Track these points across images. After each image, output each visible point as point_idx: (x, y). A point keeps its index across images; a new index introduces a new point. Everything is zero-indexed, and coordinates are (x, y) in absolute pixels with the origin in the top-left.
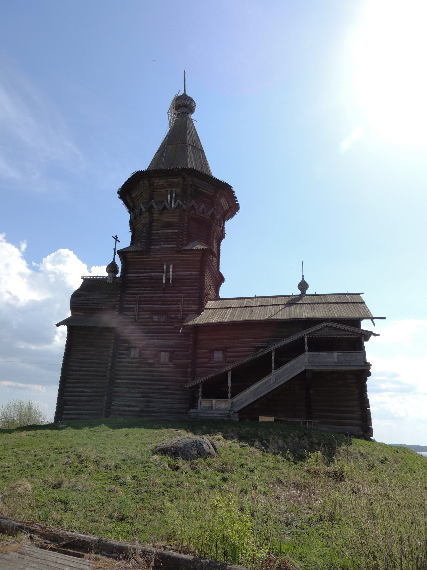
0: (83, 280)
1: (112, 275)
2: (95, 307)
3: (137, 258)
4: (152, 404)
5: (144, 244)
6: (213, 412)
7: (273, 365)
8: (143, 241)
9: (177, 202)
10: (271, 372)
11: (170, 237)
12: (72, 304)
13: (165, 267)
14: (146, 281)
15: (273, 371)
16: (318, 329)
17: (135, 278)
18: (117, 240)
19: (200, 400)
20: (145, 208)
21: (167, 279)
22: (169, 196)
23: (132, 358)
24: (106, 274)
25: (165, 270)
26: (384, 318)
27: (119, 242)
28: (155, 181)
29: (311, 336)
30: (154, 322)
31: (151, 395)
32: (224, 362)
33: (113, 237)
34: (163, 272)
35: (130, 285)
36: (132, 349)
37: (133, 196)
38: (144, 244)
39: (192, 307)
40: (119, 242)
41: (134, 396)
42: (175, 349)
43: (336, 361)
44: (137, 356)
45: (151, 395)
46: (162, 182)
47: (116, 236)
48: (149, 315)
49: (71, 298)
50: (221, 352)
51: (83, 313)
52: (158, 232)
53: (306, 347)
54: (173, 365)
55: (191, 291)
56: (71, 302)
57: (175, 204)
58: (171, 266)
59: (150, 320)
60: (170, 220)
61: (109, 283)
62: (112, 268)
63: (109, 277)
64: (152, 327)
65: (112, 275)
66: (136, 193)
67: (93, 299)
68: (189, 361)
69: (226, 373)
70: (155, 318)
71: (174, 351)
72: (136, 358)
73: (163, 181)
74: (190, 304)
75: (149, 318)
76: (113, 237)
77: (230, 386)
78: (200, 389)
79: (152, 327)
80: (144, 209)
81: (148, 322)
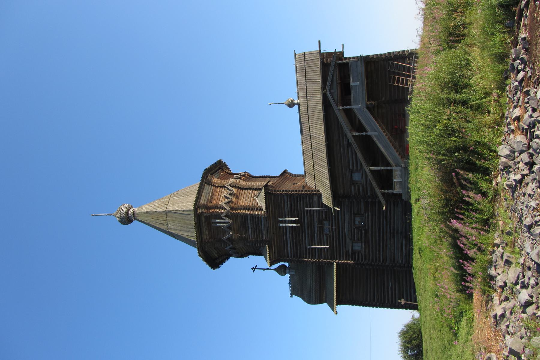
0: (293, 296)
1: (287, 271)
2: (318, 283)
3: (275, 250)
4: (399, 229)
5: (261, 245)
7: (364, 134)
8: (259, 245)
9: (223, 217)
10: (369, 135)
11: (255, 222)
12: (316, 303)
13: (281, 225)
14: (294, 240)
15: (368, 134)
16: (333, 98)
17: (292, 250)
18: (255, 268)
19: (394, 192)
20: (229, 245)
21: (292, 222)
22: (218, 225)
23: (362, 248)
24: (287, 275)
25: (284, 225)
26: (320, 42)
27: (256, 266)
28: (205, 238)
29: (339, 104)
30: (329, 231)
31: (392, 231)
32: (362, 172)
33: (253, 272)
34: (286, 227)
35: (298, 254)
36: (354, 249)
37: (216, 255)
38: (261, 245)
39: (315, 200)
40: (256, 266)
42: (352, 213)
43: (358, 83)
44: (360, 244)
45: (392, 231)
46: (206, 232)
47: (252, 269)
48: (323, 236)
49: (311, 304)
50: (353, 175)
51: (323, 292)
52: (250, 232)
53: (348, 107)
54: (366, 213)
55: (302, 201)
56: (315, 304)
57: (225, 220)
58: (281, 219)
59: (328, 235)
60: (239, 223)
61: (295, 273)
62: (282, 271)
63: (289, 273)
64: (334, 233)
65: (288, 270)
66: (214, 253)
67: (311, 285)
68: (362, 200)
69: (372, 171)
70: (326, 231)
71: (354, 214)
72: (362, 245)
73: (204, 231)
74: (313, 202)
75: (327, 236)
76: (253, 272)
77: (382, 168)
78: (386, 191)
79: (334, 233)
80: (231, 246)
81: (330, 236)
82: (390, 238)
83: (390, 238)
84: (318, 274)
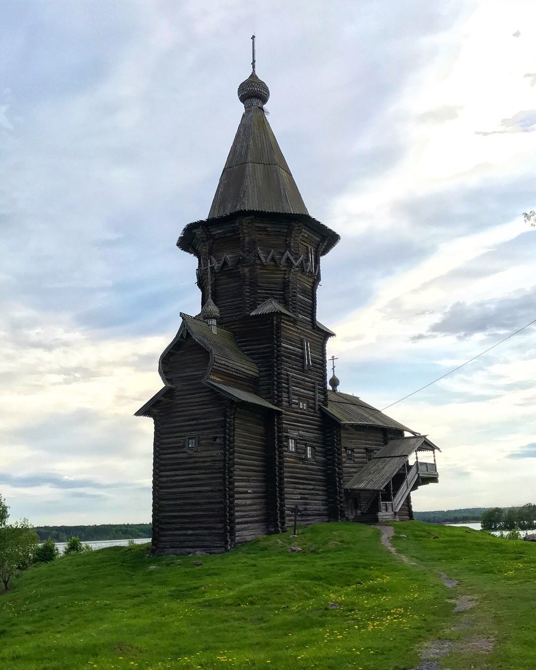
30: (301, 409)
41: (296, 498)
46: (307, 234)
82: (300, 494)
83: (300, 494)
84: (244, 377)
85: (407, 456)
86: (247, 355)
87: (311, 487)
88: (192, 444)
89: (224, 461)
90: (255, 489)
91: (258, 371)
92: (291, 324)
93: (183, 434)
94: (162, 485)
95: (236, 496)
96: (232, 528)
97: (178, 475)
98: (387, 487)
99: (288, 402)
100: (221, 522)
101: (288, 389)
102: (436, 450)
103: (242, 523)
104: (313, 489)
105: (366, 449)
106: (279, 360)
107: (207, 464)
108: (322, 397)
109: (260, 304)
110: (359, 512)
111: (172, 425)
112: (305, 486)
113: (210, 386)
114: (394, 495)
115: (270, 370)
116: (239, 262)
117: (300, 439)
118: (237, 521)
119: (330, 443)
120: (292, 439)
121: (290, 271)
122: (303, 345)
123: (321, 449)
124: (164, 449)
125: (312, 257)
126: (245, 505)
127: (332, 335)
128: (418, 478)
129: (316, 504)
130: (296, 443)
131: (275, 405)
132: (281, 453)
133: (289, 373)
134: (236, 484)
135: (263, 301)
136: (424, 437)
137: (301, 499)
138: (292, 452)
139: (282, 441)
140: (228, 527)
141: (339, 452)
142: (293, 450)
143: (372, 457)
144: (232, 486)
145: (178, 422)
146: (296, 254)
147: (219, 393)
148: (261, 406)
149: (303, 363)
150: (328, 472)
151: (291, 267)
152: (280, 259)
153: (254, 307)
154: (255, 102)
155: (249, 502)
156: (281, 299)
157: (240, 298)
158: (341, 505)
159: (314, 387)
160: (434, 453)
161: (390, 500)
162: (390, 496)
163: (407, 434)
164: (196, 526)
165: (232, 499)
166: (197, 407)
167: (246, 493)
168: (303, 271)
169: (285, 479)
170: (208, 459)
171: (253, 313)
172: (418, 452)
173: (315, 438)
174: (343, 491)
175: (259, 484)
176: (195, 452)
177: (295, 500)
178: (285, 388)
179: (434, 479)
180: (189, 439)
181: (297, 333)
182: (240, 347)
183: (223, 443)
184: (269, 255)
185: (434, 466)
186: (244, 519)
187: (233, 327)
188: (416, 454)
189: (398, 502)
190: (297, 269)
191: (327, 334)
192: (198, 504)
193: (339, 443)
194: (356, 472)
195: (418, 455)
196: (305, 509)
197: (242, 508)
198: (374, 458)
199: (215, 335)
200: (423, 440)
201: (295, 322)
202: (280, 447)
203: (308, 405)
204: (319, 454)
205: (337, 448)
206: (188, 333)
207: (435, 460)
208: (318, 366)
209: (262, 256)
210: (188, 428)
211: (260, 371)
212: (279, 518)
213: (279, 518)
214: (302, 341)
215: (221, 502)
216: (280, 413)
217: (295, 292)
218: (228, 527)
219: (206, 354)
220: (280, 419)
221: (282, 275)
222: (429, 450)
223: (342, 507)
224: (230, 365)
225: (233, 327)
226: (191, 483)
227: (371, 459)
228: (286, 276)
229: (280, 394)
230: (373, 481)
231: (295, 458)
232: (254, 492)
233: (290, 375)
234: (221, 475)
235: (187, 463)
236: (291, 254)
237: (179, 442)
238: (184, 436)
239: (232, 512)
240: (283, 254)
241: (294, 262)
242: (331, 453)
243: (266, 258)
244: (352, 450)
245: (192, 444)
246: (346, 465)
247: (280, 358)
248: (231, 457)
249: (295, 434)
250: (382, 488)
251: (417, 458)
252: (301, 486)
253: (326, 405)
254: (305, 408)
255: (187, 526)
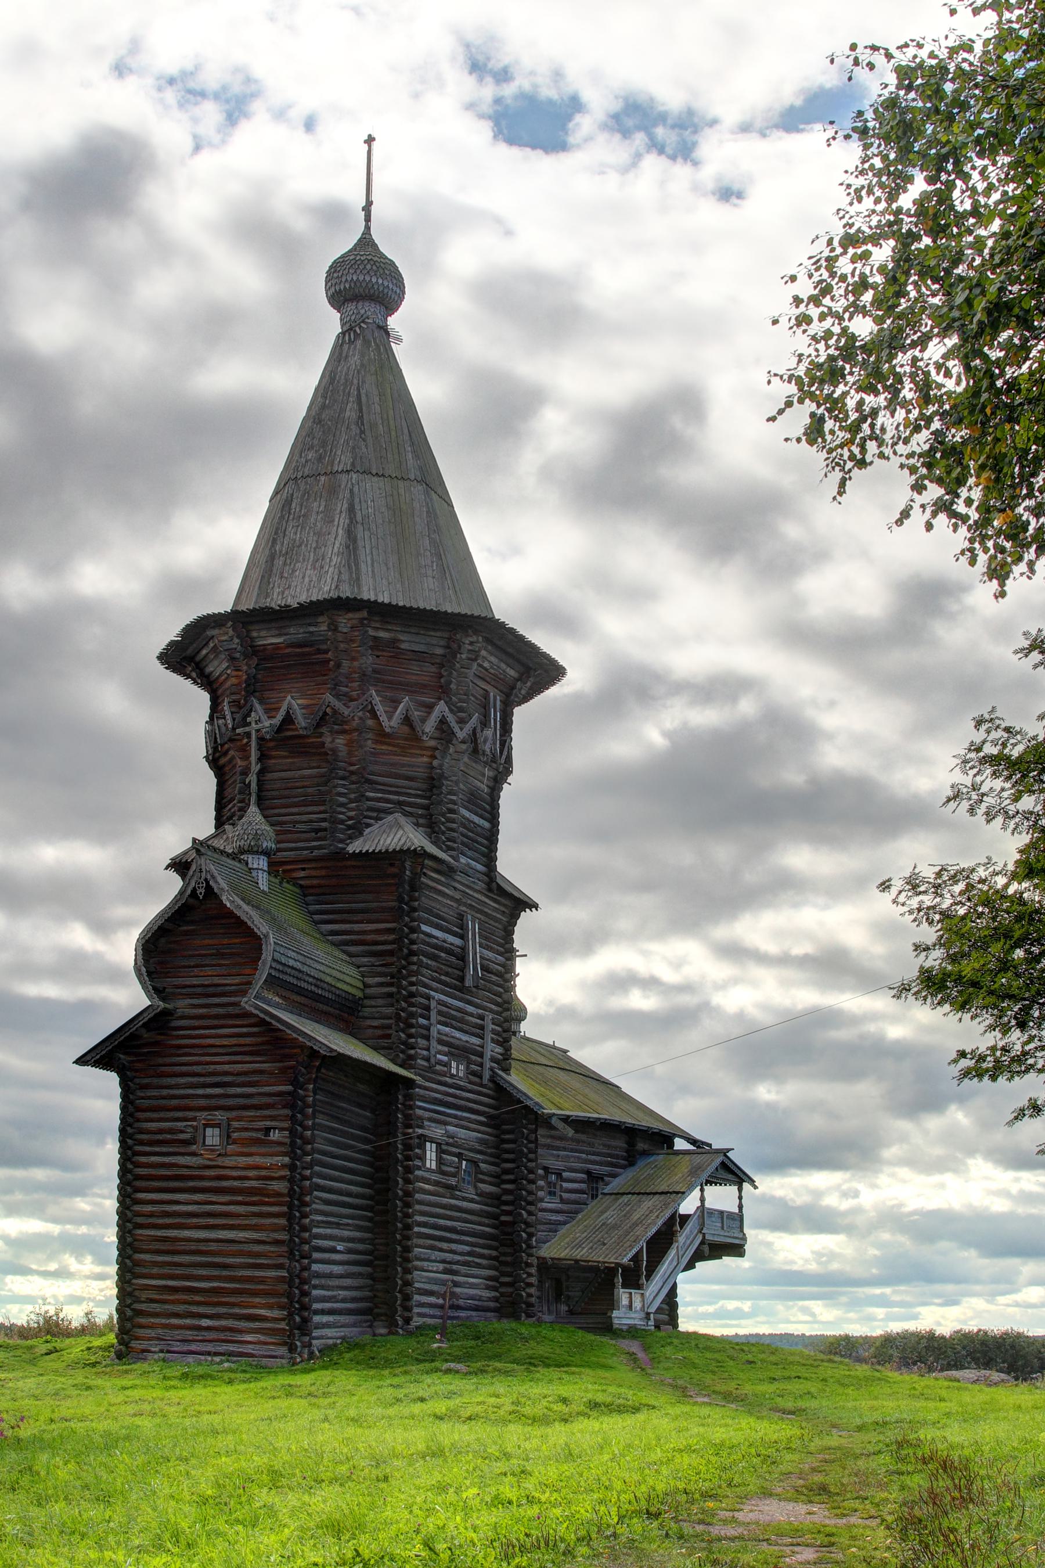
2: (313, 988)
6: (633, 1315)
30: (452, 1076)
31: (454, 1267)
45: (454, 1267)
46: (490, 662)
54: (477, 1194)
73: (493, 659)
82: (443, 1261)
83: (443, 1261)
85: (683, 1193)
86: (333, 944)
87: (467, 1248)
88: (213, 1137)
89: (291, 1180)
90: (350, 1245)
91: (360, 985)
92: (443, 879)
93: (190, 1114)
94: (139, 1220)
95: (316, 1255)
96: (305, 1321)
97: (178, 1203)
98: (636, 1258)
99: (428, 1060)
100: (281, 1307)
101: (428, 1029)
102: (746, 1186)
103: (323, 1312)
104: (469, 1254)
105: (588, 1173)
106: (414, 964)
107: (248, 1184)
108: (499, 1050)
109: (368, 825)
110: (564, 1308)
111: (165, 1092)
112: (454, 1246)
113: (262, 1015)
114: (648, 1277)
115: (391, 985)
116: (323, 720)
117: (447, 1144)
118: (316, 1306)
119: (512, 1156)
120: (432, 1142)
121: (445, 752)
122: (463, 927)
123: (492, 1168)
124: (142, 1143)
125: (495, 716)
126: (330, 1276)
127: (533, 906)
128: (702, 1243)
129: (472, 1286)
130: (440, 1151)
131: (401, 1066)
132: (409, 1170)
133: (432, 993)
134: (315, 1230)
135: (377, 819)
136: (725, 1152)
137: (446, 1271)
138: (429, 1170)
139: (414, 1147)
140: (298, 1319)
141: (531, 1176)
142: (434, 1167)
143: (600, 1191)
144: (308, 1234)
145: (177, 1086)
146: (461, 710)
147: (281, 1030)
148: (365, 1063)
149: (463, 969)
150: (503, 1218)
151: (449, 741)
152: (423, 721)
153: (357, 830)
154: (369, 309)
155: (337, 1269)
156: (421, 816)
157: (322, 808)
158: (528, 1290)
159: (482, 1028)
160: (740, 1190)
161: (639, 1287)
162: (639, 1277)
163: (680, 1144)
164: (222, 1310)
165: (306, 1261)
166: (227, 1058)
167: (333, 1250)
168: (475, 751)
169: (416, 1229)
170: (251, 1173)
171: (356, 846)
172: (708, 1189)
173: (481, 1141)
174: (534, 1261)
175: (358, 1234)
176: (219, 1155)
177: (432, 1275)
178: (422, 1027)
179: (736, 1249)
180: (206, 1126)
181: (452, 898)
182: (316, 923)
183: (288, 1141)
184: (396, 708)
185: (738, 1218)
186: (327, 1305)
187: (302, 874)
188: (702, 1190)
189: (654, 1289)
190: (464, 747)
191: (520, 904)
192: (225, 1266)
193: (531, 1156)
194: (565, 1223)
195: (706, 1194)
196: (453, 1295)
197: (323, 1281)
198: (602, 1194)
199: (263, 892)
200: (721, 1158)
201: (448, 871)
202: (408, 1158)
203: (467, 1068)
204: (486, 1178)
205: (526, 1167)
206: (209, 889)
207: (740, 1207)
208: (494, 978)
209: (380, 709)
210: (202, 1102)
211: (366, 986)
212: (399, 1308)
213: (399, 1308)
214: (461, 917)
215: (280, 1267)
216: (409, 1083)
217: (454, 803)
218: (298, 1319)
219: (254, 942)
220: (408, 1097)
221: (425, 759)
222: (732, 1183)
223: (530, 1295)
224: (305, 969)
225: (302, 874)
226: (212, 1221)
227: (597, 1196)
228: (435, 763)
229: (413, 1040)
230: (604, 1244)
231: (437, 1183)
232: (349, 1251)
233: (434, 998)
234: (285, 1209)
235: (201, 1178)
236: (451, 711)
237: (182, 1132)
238: (194, 1119)
239: (306, 1287)
240: (430, 707)
241: (456, 729)
242: (511, 1177)
243: (390, 718)
244: (559, 1175)
245: (213, 1137)
246: (544, 1205)
247: (415, 959)
248: (308, 1172)
249: (437, 1132)
250: (625, 1261)
251: (702, 1200)
252: (445, 1245)
253: (507, 1070)
254: (461, 1074)
255: (201, 1310)
